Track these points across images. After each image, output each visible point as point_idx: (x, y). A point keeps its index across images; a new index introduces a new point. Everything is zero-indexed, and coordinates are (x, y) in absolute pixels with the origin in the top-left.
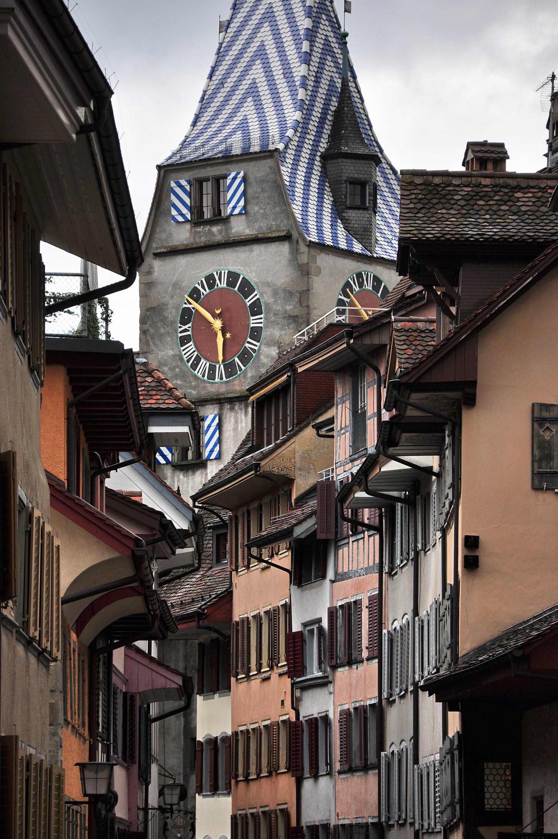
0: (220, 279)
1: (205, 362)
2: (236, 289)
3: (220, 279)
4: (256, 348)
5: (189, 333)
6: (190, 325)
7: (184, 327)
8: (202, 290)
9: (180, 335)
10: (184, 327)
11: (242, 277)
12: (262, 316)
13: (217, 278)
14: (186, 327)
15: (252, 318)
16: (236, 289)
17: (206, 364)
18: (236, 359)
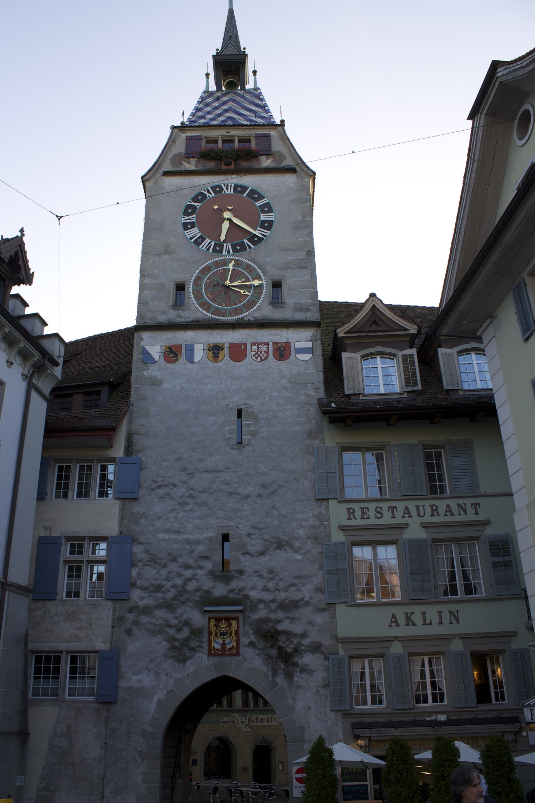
0: (227, 189)
1: (209, 241)
2: (245, 195)
3: (227, 189)
4: (267, 234)
5: (194, 221)
6: (194, 216)
7: (187, 218)
8: (208, 194)
9: (183, 222)
10: (187, 218)
11: (250, 189)
12: (273, 214)
13: (224, 188)
14: (190, 217)
15: (262, 215)
16: (245, 195)
17: (210, 242)
18: (245, 241)
